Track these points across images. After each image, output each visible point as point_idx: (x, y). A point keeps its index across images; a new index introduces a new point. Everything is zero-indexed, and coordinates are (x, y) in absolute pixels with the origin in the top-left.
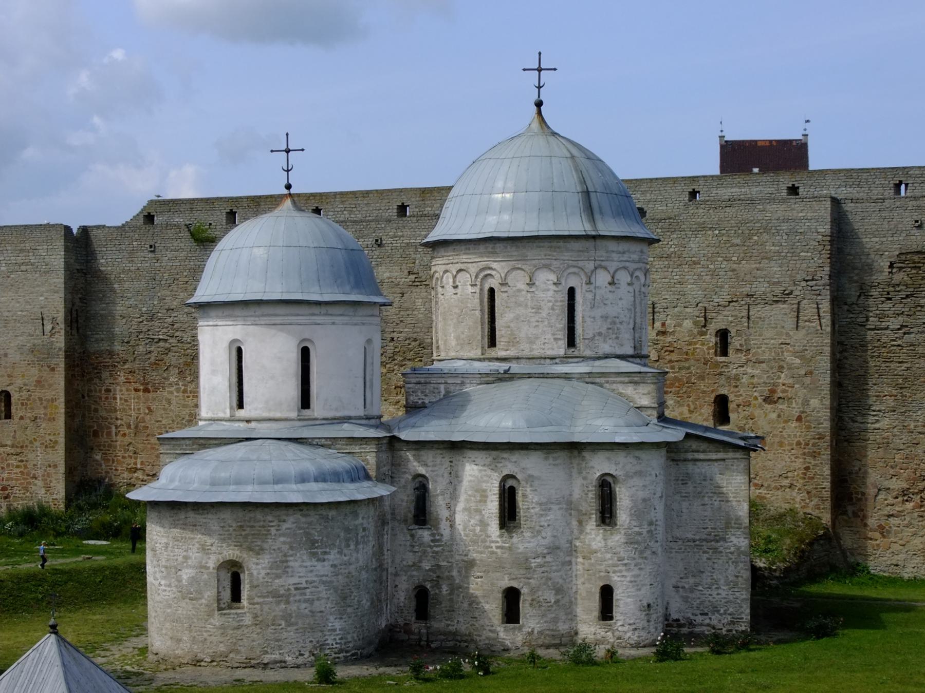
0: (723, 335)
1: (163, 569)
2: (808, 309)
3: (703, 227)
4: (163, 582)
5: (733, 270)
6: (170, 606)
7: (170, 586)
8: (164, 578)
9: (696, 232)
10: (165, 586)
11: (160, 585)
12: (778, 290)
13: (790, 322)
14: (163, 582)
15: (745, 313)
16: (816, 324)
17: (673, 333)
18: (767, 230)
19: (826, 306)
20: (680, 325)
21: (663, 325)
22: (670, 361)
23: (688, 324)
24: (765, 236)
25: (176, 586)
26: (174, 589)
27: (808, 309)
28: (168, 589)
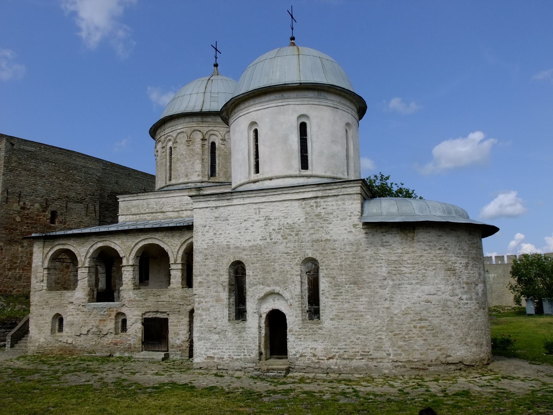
0: (54, 215)
1: (465, 285)
2: (91, 208)
3: (47, 160)
4: (464, 297)
5: (61, 184)
6: (471, 317)
7: (471, 299)
8: (466, 293)
9: (44, 162)
10: (466, 299)
11: (461, 299)
12: (79, 197)
13: (83, 213)
14: (464, 297)
15: (65, 205)
16: (94, 215)
17: (29, 209)
18: (76, 169)
19: (97, 208)
20: (33, 205)
21: (24, 204)
22: (27, 223)
23: (37, 205)
24: (75, 172)
25: (476, 299)
26: (474, 301)
27: (91, 208)
28: (469, 302)
